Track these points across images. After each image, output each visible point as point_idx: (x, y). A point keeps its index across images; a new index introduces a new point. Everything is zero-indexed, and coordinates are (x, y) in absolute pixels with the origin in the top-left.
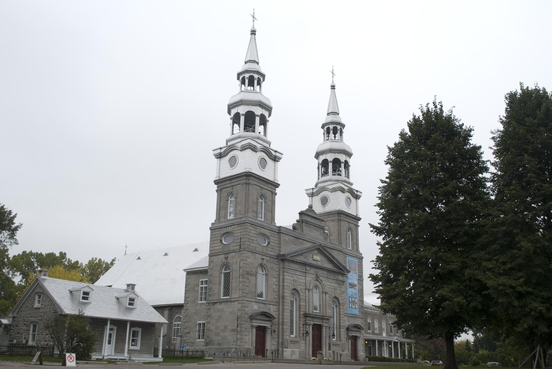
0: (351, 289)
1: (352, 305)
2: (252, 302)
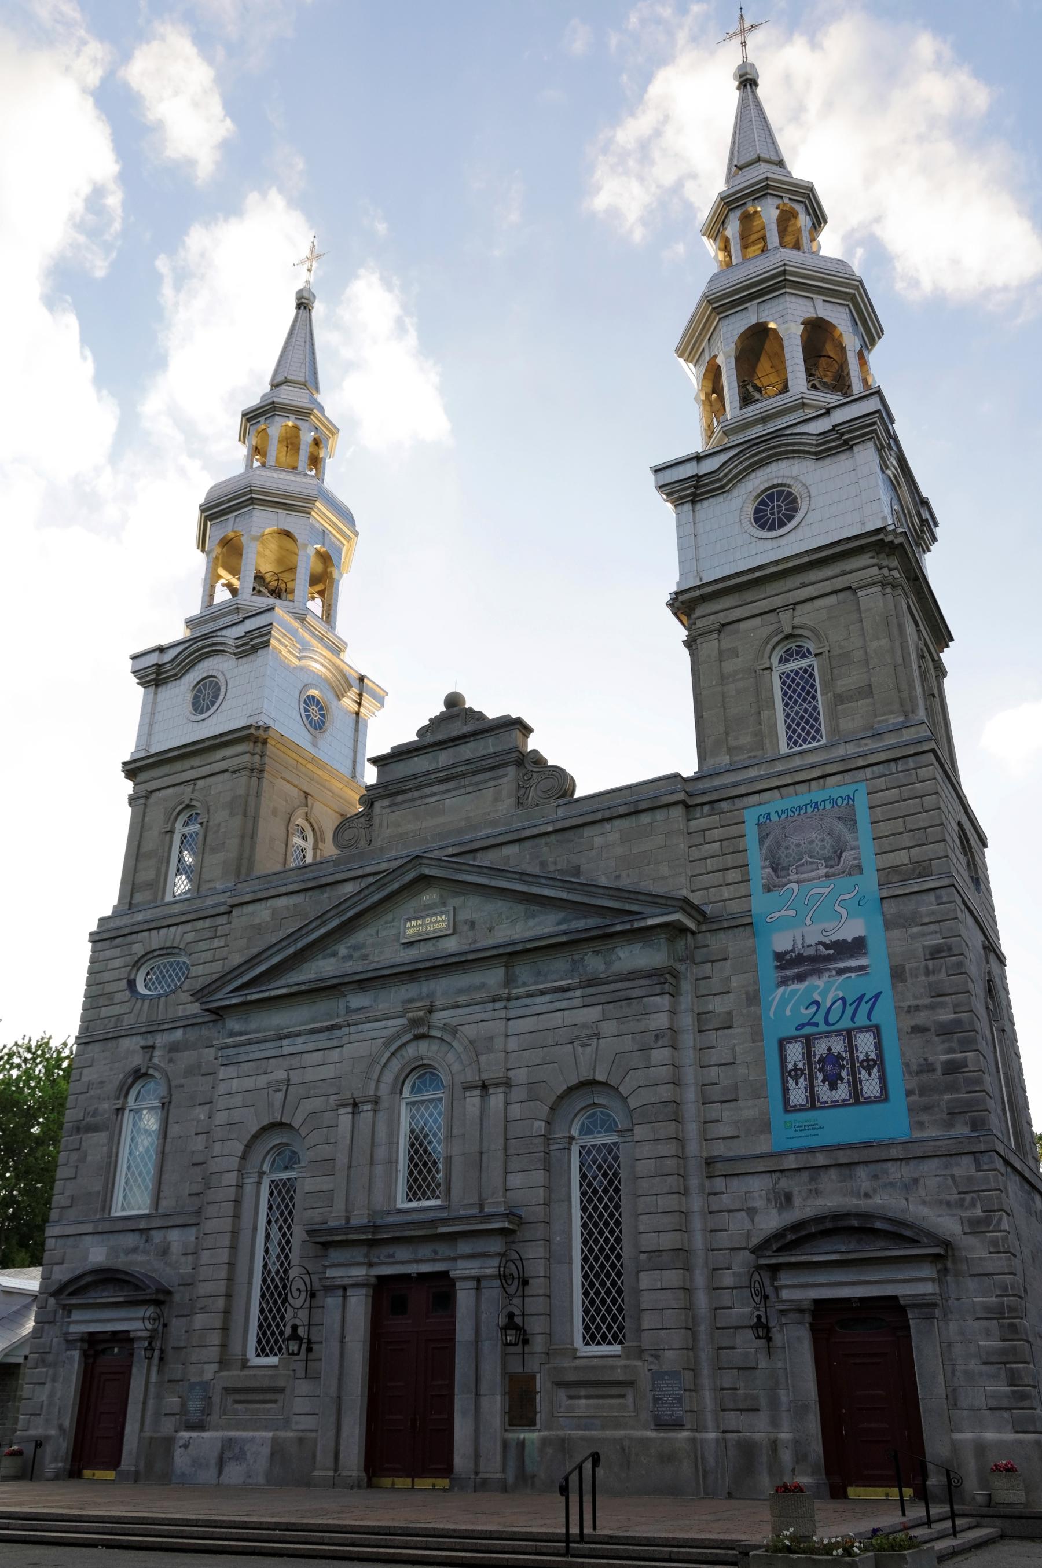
0: (801, 987)
1: (811, 1087)
2: (84, 1237)
